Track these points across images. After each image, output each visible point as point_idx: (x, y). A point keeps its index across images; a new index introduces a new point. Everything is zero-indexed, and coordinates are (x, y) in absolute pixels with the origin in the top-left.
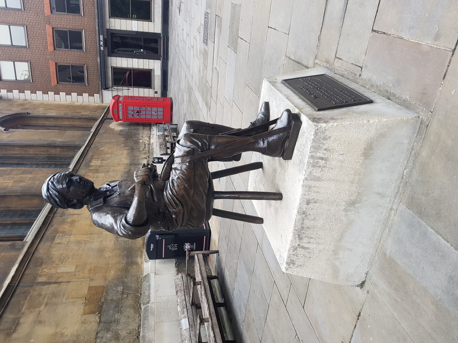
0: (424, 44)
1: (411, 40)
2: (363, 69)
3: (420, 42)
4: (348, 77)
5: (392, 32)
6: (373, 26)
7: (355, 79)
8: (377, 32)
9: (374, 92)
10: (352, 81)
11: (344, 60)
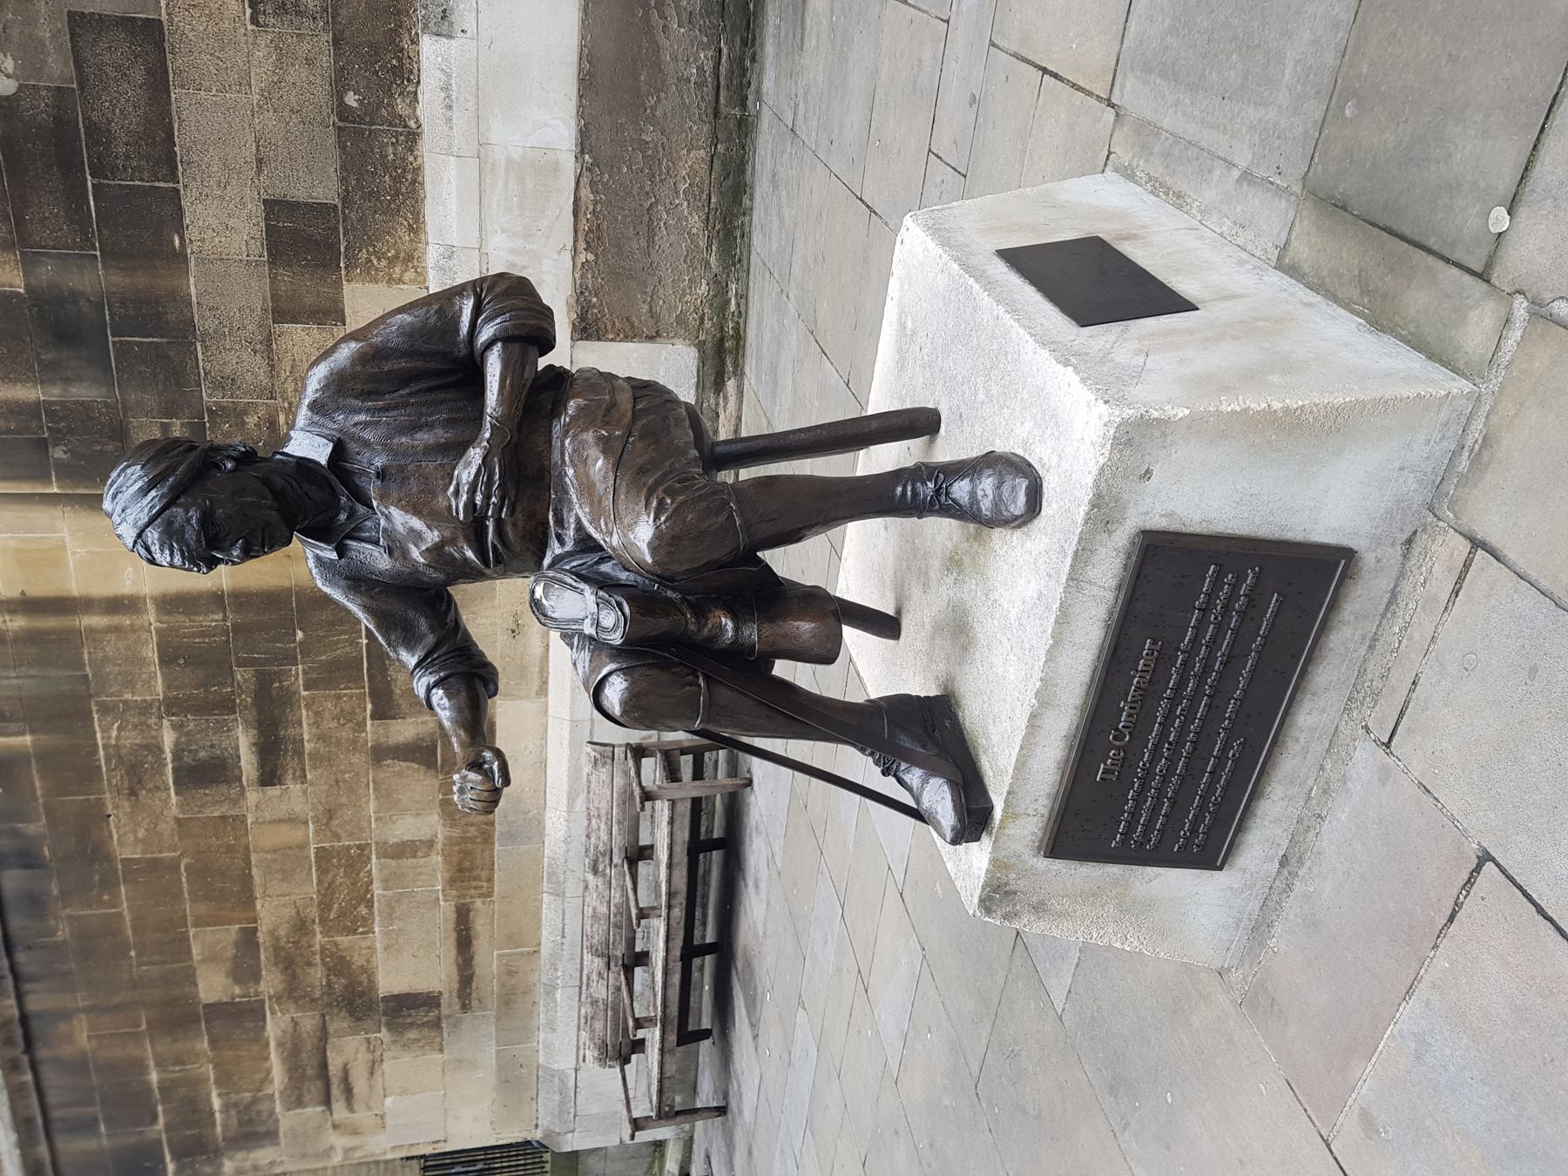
1: (1390, 1028)
2: (1380, 752)
5: (1441, 962)
7: (1360, 696)
9: (1309, 798)
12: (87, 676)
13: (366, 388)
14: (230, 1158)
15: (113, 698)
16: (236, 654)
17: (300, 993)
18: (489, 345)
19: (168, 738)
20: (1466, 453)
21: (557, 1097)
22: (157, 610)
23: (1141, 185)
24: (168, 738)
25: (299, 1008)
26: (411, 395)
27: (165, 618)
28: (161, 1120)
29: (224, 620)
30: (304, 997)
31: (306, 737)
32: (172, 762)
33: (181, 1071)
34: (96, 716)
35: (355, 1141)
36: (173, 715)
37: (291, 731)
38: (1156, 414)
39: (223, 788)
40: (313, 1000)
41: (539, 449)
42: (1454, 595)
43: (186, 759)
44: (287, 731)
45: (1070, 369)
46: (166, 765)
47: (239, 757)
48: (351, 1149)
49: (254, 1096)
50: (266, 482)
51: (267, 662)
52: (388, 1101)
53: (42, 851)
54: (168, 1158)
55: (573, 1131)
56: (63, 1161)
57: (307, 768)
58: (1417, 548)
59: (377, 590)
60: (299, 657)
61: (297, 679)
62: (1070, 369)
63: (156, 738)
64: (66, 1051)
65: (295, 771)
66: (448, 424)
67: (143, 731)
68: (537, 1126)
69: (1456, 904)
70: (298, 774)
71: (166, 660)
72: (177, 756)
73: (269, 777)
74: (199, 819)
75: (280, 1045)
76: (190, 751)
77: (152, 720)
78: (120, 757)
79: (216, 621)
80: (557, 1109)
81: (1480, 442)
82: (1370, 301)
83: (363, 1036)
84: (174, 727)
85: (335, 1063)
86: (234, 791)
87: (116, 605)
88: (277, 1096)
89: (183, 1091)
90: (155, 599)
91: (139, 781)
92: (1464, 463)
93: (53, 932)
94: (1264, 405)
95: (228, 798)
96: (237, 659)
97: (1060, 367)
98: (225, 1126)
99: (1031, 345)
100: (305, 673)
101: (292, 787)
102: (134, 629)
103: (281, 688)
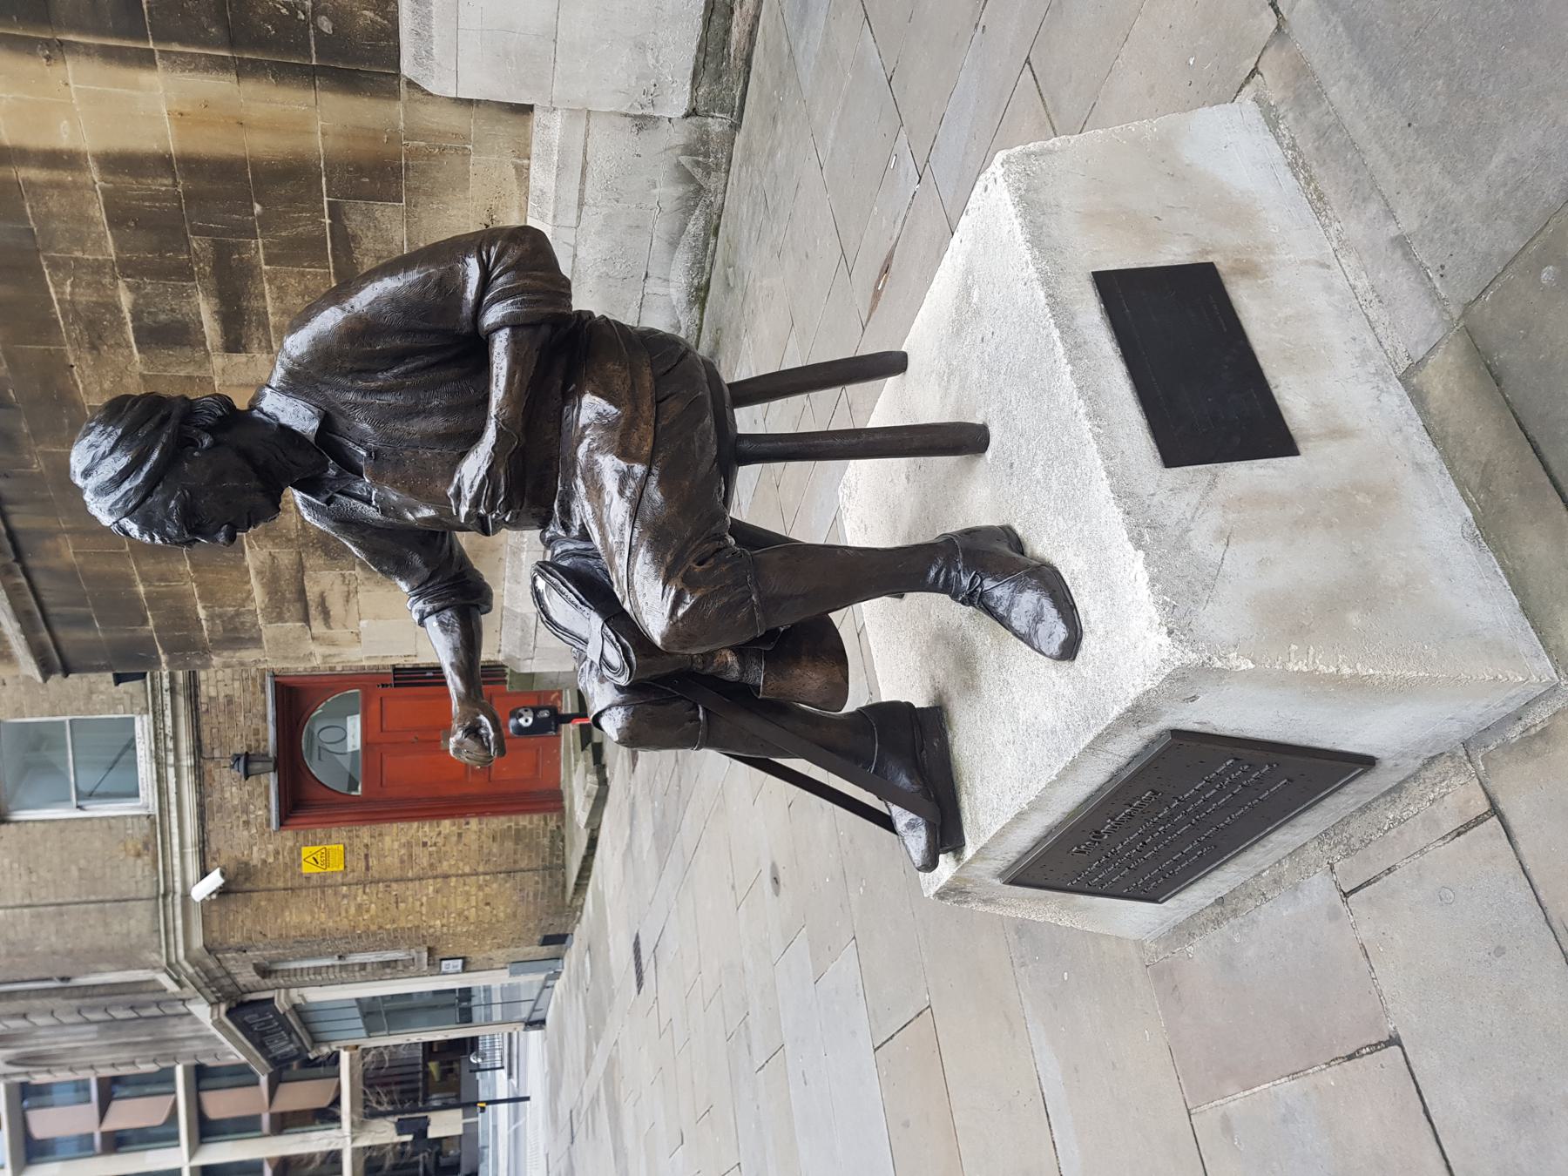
0: (1238, 1095)
2: (1337, 895)
3: (1247, 1093)
4: (1369, 816)
6: (1404, 1054)
7: (1336, 839)
8: (1376, 1045)
9: (1259, 875)
10: (1344, 822)
11: (1441, 843)
12: (32, 230)
13: (356, 366)
14: (218, 655)
15: (62, 255)
16: (190, 221)
17: (275, 533)
18: (497, 328)
19: (125, 300)
20: (1519, 728)
21: (519, 633)
22: (101, 168)
23: (1281, 144)
24: (125, 300)
25: (275, 545)
26: (406, 374)
27: (111, 178)
28: (151, 622)
29: (175, 185)
30: (281, 537)
31: (270, 310)
32: (132, 322)
33: (166, 586)
34: (47, 271)
35: (333, 650)
36: (128, 277)
37: (255, 304)
38: (1218, 664)
39: (188, 351)
40: (290, 540)
41: (547, 438)
42: (1455, 833)
43: (145, 320)
44: (249, 302)
45: (1141, 554)
46: (125, 324)
47: (201, 323)
48: (330, 655)
49: (238, 610)
50: (246, 455)
51: (224, 233)
52: (363, 623)
53: (7, 393)
54: (160, 651)
55: (532, 659)
56: (64, 646)
57: (273, 339)
58: (1437, 768)
59: (369, 532)
60: (258, 230)
61: (257, 252)
62: (1141, 554)
63: (113, 297)
64: (54, 563)
65: (260, 341)
66: (448, 411)
67: (98, 290)
68: (499, 651)
69: (1358, 1051)
70: (263, 344)
71: (115, 221)
72: (136, 315)
73: (234, 344)
74: (165, 376)
75: (259, 573)
76: (149, 313)
77: (107, 280)
78: (76, 313)
79: (165, 186)
80: (518, 642)
81: (1538, 729)
82: (1486, 501)
83: (338, 572)
84: (129, 287)
85: (312, 591)
86: (198, 355)
87: (54, 159)
88: (258, 611)
89: (170, 602)
90: (96, 157)
91: (100, 337)
92: (1514, 733)
93: (29, 465)
94: (1333, 669)
95: (193, 360)
96: (191, 226)
97: (1129, 546)
98: (211, 631)
99: (1102, 488)
100: (264, 246)
101: (258, 355)
102: (75, 185)
103: (241, 260)
